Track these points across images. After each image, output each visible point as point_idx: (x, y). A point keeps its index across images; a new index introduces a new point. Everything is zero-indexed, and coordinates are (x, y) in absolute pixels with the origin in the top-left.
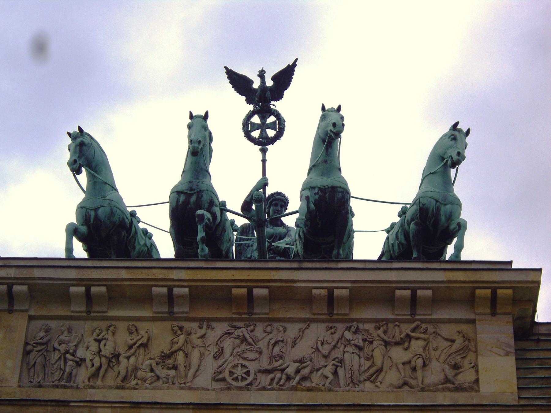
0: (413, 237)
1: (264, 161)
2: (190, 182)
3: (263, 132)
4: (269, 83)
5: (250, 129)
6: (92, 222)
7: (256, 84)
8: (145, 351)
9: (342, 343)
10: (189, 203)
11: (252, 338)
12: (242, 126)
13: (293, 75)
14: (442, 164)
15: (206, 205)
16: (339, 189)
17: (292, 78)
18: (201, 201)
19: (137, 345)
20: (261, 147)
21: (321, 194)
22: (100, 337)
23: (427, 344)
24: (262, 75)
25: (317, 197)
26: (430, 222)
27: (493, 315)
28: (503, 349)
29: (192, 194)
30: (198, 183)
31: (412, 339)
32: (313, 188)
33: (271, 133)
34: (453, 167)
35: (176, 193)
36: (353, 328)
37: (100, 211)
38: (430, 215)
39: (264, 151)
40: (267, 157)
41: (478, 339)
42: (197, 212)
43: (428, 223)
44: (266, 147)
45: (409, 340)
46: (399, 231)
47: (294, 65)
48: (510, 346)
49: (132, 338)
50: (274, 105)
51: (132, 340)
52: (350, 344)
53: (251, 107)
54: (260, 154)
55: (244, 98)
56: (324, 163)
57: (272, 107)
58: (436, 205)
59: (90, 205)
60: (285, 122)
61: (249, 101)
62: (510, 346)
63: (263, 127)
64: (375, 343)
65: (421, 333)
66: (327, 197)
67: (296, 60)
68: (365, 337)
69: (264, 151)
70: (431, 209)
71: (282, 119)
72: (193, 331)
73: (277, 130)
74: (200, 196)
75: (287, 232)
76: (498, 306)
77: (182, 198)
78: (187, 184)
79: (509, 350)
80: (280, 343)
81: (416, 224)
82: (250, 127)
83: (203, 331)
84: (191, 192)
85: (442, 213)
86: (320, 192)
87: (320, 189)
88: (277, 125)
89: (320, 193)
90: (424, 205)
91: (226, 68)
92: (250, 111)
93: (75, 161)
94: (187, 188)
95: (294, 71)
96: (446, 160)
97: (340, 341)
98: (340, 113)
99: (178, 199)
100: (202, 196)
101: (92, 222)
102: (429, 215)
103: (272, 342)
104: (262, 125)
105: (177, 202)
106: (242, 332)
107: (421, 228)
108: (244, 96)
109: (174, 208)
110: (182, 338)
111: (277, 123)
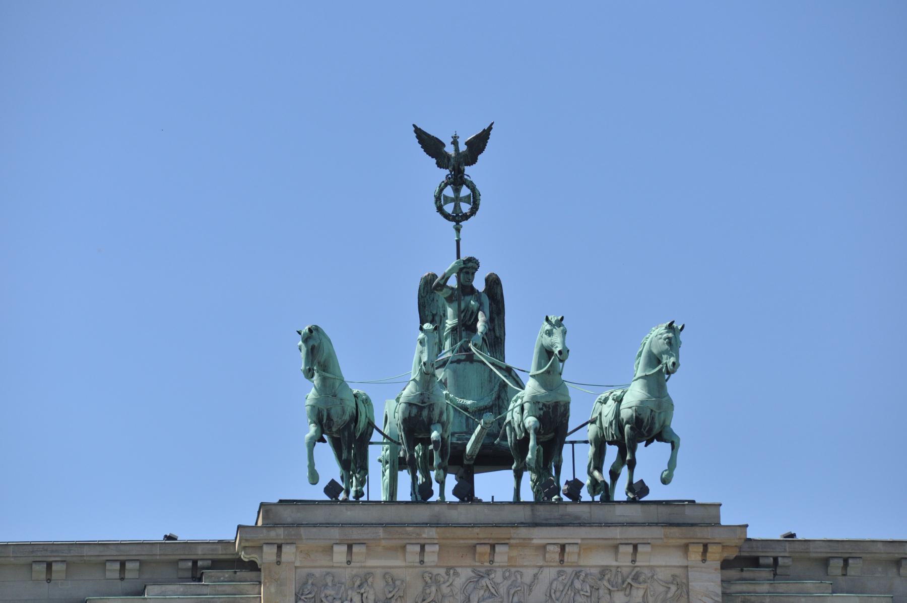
0: (629, 439)
1: (458, 242)
2: (421, 394)
3: (457, 207)
4: (463, 148)
5: (442, 202)
6: (325, 421)
7: (450, 149)
8: (401, 601)
9: (571, 590)
10: (421, 415)
11: (494, 588)
12: (433, 199)
13: (489, 138)
14: (657, 369)
15: (437, 418)
16: (562, 403)
17: (487, 142)
18: (433, 415)
19: (395, 598)
20: (455, 223)
21: (546, 410)
22: (362, 591)
23: (645, 593)
24: (455, 143)
25: (541, 412)
26: (644, 430)
27: (704, 561)
28: (712, 599)
29: (424, 407)
30: (429, 395)
31: (633, 588)
32: (539, 402)
33: (465, 208)
34: (667, 374)
35: (408, 405)
36: (581, 576)
37: (333, 412)
38: (645, 424)
39: (458, 230)
40: (461, 237)
41: (690, 587)
42: (432, 437)
43: (643, 430)
44: (460, 224)
45: (630, 586)
46: (614, 422)
47: (490, 128)
48: (717, 595)
49: (391, 589)
50: (468, 176)
51: (390, 592)
52: (579, 592)
53: (443, 174)
54: (454, 232)
55: (434, 160)
56: (547, 374)
57: (466, 177)
58: (651, 414)
59: (322, 406)
60: (480, 195)
61: (440, 165)
62: (717, 595)
63: (457, 200)
64: (601, 592)
65: (640, 583)
66: (551, 412)
67: (492, 123)
68: (592, 585)
69: (458, 230)
70: (646, 420)
71: (477, 192)
72: (442, 580)
73: (472, 204)
74: (431, 409)
75: (479, 305)
76: (708, 554)
77: (414, 411)
78: (418, 396)
79: (716, 599)
80: (518, 592)
81: (631, 428)
82: (442, 200)
83: (451, 581)
84: (423, 405)
85: (657, 421)
86: (544, 407)
87: (544, 405)
88: (472, 198)
89: (545, 409)
90: (639, 414)
91: (414, 126)
92: (443, 182)
93: (310, 370)
94: (418, 401)
95: (489, 134)
96: (661, 366)
97: (570, 589)
98: (563, 322)
99: (410, 411)
100: (433, 409)
101: (325, 421)
102: (644, 425)
103: (512, 592)
104: (455, 200)
105: (410, 413)
106: (486, 582)
107: (636, 433)
108: (434, 159)
109: (405, 418)
110: (433, 589)
111: (472, 195)
